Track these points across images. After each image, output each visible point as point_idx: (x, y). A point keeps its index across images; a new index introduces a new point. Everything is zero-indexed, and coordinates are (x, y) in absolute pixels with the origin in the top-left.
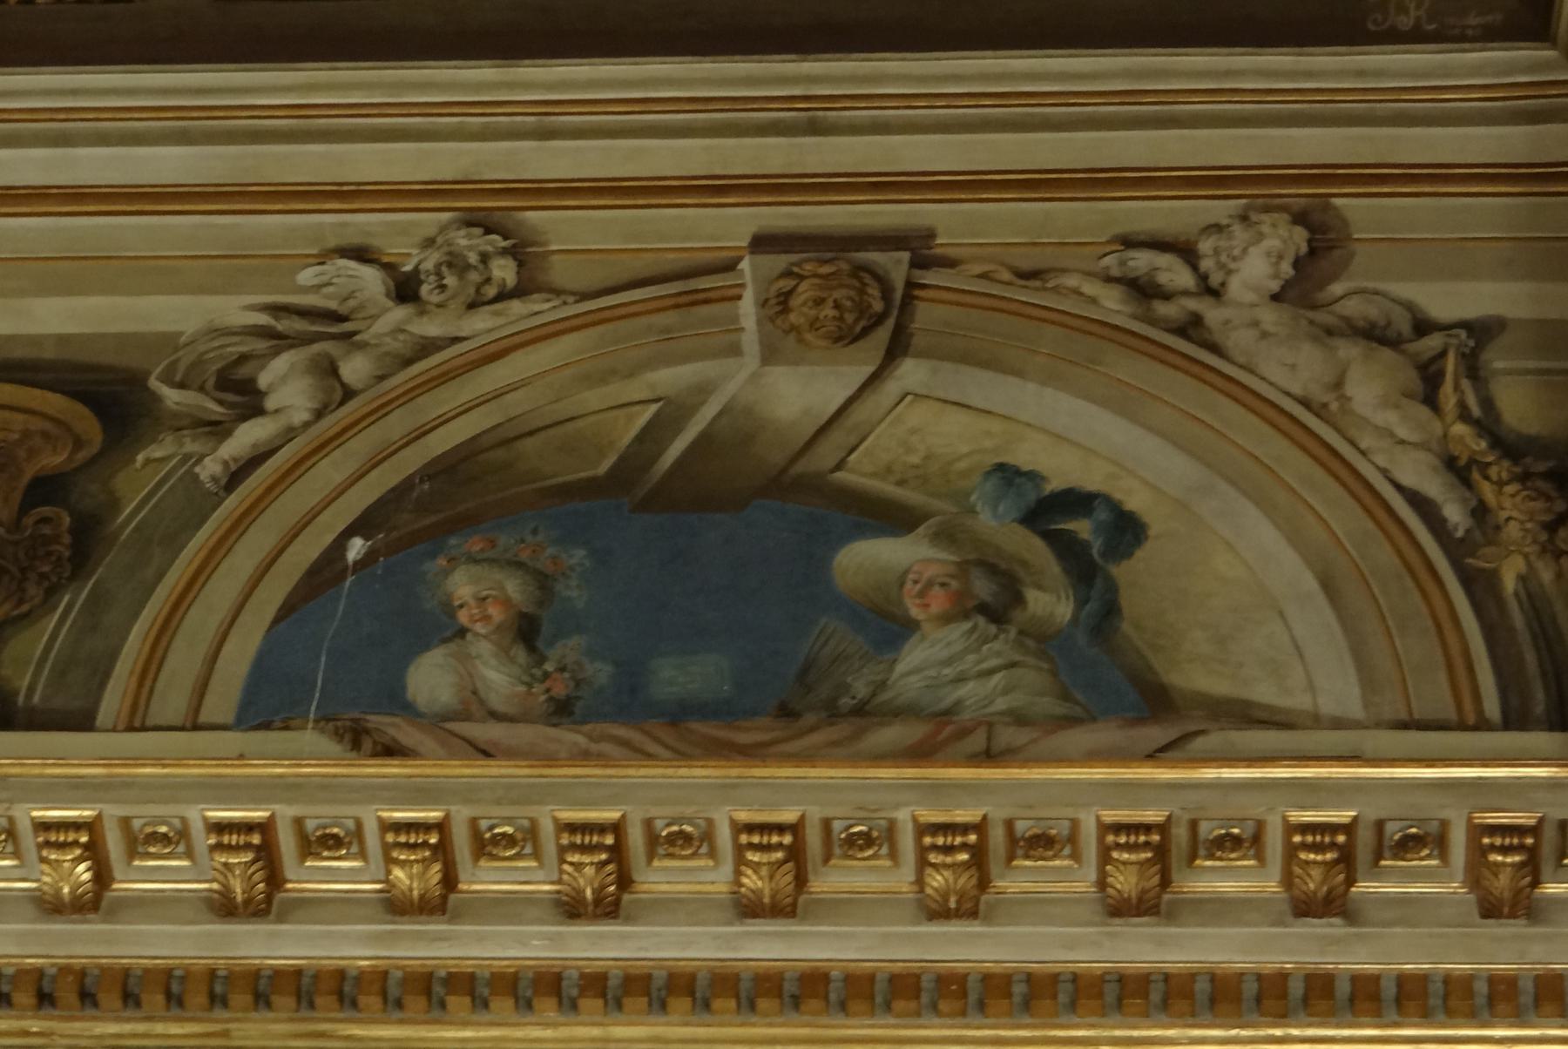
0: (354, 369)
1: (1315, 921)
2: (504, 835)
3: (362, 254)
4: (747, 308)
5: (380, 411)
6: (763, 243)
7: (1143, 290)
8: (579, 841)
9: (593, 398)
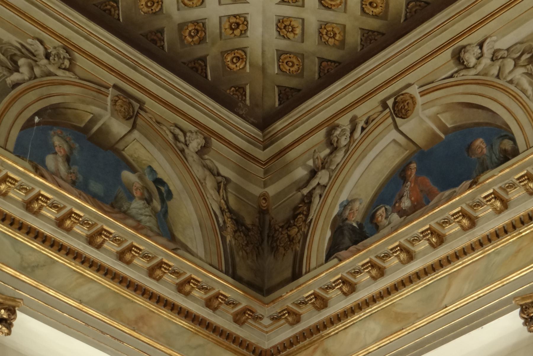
0: (37, 71)
1: (209, 309)
2: (205, 288)
3: (41, 42)
4: (109, 99)
5: (41, 85)
6: (115, 87)
7: (176, 138)
8: (105, 234)
9: (82, 106)
